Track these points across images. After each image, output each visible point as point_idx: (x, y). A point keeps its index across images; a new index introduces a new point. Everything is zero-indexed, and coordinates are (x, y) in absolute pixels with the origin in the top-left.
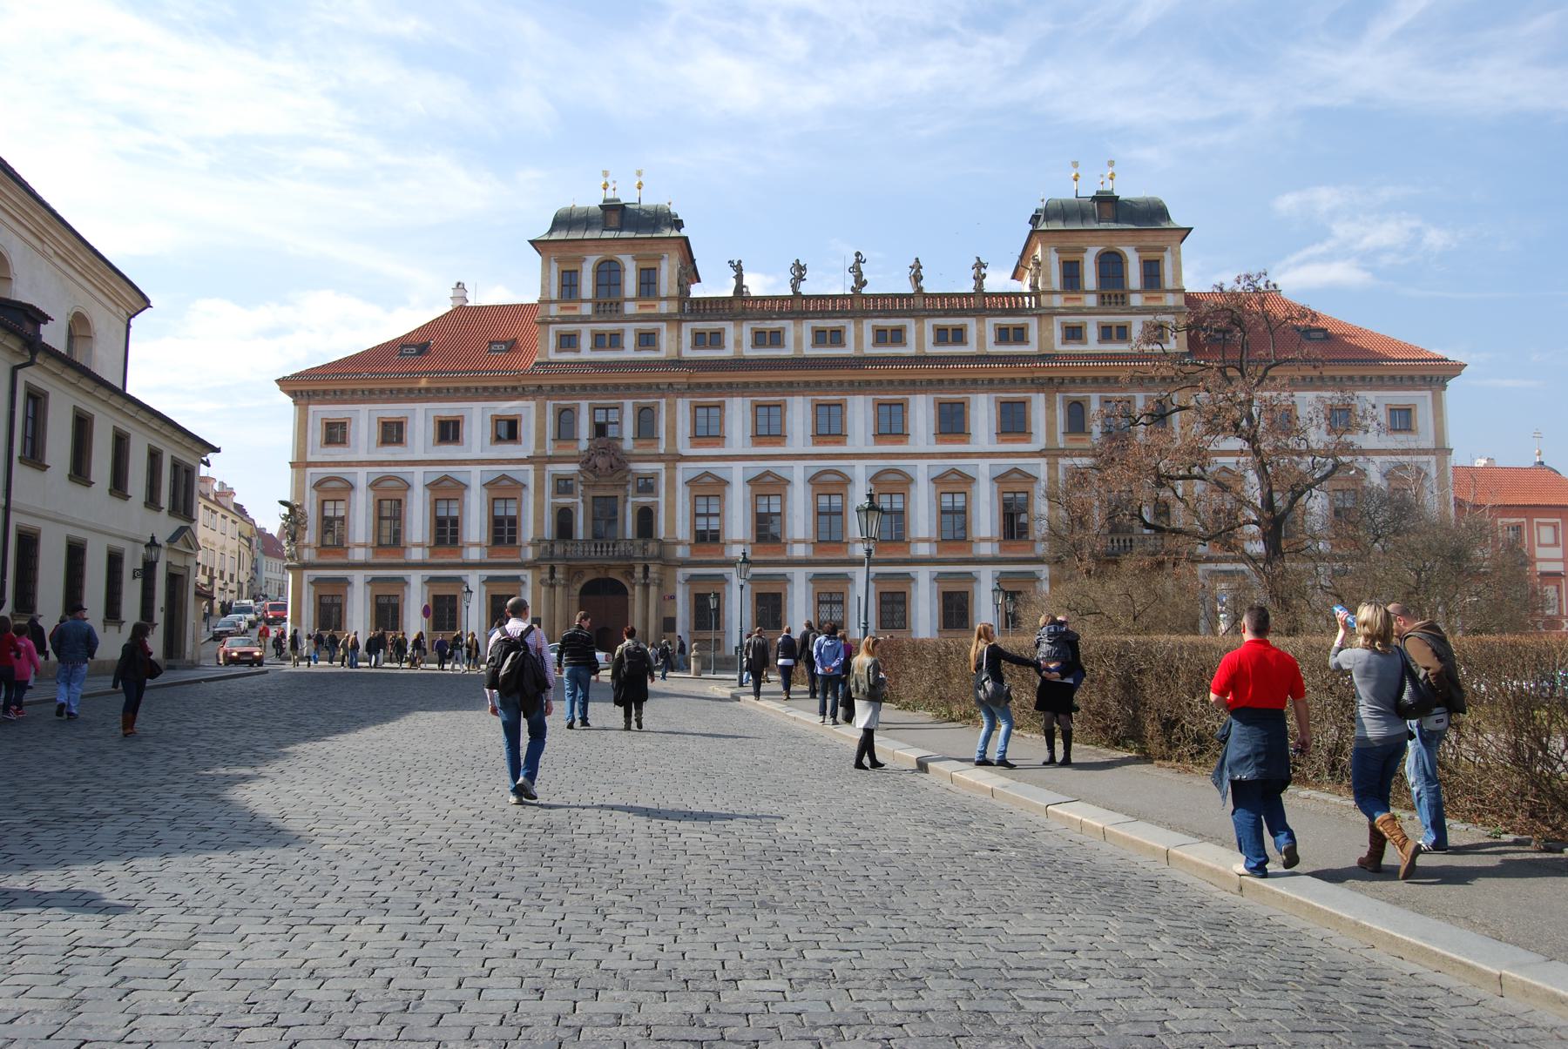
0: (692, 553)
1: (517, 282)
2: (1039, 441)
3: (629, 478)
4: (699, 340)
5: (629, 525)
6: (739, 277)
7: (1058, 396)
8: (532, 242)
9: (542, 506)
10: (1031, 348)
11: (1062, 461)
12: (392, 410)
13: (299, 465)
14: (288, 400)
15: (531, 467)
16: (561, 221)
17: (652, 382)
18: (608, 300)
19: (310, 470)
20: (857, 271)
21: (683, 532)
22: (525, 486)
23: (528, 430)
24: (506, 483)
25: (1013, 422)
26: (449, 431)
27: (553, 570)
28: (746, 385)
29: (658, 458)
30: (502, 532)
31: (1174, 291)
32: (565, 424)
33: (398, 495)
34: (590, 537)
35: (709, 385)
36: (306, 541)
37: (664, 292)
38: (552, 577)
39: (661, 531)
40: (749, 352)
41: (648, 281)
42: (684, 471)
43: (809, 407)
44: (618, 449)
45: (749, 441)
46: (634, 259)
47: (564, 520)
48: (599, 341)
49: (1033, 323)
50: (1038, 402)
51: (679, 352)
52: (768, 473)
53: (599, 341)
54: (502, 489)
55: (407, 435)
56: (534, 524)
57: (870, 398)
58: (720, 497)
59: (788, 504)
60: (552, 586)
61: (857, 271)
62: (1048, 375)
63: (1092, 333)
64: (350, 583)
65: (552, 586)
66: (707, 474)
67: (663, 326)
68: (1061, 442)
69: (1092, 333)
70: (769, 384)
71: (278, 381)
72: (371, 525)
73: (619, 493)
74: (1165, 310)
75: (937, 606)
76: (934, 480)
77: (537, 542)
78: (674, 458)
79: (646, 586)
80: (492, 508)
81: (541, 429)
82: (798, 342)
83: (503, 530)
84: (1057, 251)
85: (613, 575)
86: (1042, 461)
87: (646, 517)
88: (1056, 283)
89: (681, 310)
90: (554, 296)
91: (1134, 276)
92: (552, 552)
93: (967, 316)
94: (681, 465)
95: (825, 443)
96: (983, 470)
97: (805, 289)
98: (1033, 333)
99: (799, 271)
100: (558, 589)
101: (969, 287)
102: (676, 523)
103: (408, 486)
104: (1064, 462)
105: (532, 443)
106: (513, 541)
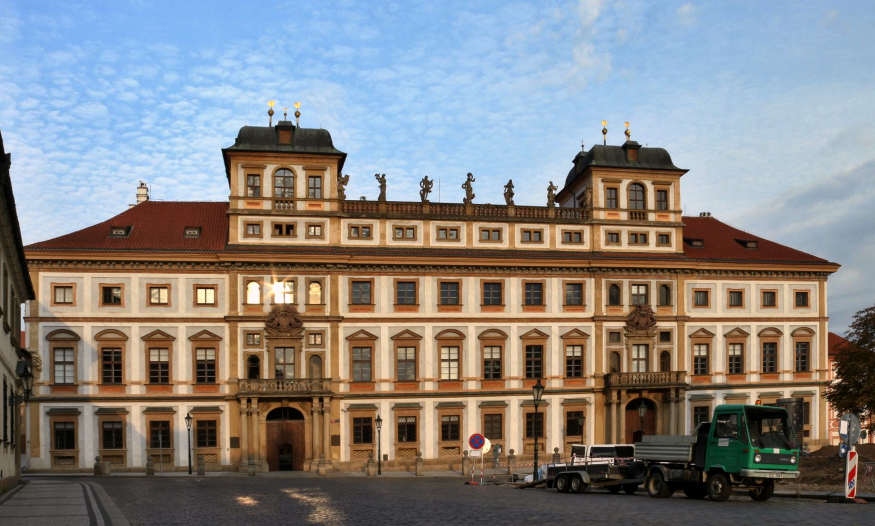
0: (351, 389)
3: (303, 334)
7: (604, 281)
9: (236, 355)
10: (586, 247)
12: (110, 278)
15: (226, 325)
18: (284, 201)
21: (344, 373)
24: (205, 336)
25: (575, 298)
27: (249, 401)
29: (326, 319)
31: (675, 212)
34: (273, 377)
36: (41, 380)
37: (327, 195)
39: (328, 374)
42: (344, 330)
43: (436, 284)
44: (296, 313)
45: (392, 308)
47: (253, 363)
49: (587, 230)
50: (590, 284)
51: (339, 241)
52: (407, 331)
56: (230, 369)
57: (479, 278)
58: (371, 349)
59: (421, 353)
60: (249, 414)
62: (595, 264)
63: (625, 238)
64: (79, 413)
65: (249, 414)
66: (363, 332)
69: (625, 238)
73: (296, 345)
77: (234, 382)
78: (336, 320)
79: (322, 413)
80: (195, 355)
83: (205, 373)
94: (342, 325)
95: (448, 310)
96: (514, 332)
102: (340, 367)
103: (125, 338)
105: (227, 306)
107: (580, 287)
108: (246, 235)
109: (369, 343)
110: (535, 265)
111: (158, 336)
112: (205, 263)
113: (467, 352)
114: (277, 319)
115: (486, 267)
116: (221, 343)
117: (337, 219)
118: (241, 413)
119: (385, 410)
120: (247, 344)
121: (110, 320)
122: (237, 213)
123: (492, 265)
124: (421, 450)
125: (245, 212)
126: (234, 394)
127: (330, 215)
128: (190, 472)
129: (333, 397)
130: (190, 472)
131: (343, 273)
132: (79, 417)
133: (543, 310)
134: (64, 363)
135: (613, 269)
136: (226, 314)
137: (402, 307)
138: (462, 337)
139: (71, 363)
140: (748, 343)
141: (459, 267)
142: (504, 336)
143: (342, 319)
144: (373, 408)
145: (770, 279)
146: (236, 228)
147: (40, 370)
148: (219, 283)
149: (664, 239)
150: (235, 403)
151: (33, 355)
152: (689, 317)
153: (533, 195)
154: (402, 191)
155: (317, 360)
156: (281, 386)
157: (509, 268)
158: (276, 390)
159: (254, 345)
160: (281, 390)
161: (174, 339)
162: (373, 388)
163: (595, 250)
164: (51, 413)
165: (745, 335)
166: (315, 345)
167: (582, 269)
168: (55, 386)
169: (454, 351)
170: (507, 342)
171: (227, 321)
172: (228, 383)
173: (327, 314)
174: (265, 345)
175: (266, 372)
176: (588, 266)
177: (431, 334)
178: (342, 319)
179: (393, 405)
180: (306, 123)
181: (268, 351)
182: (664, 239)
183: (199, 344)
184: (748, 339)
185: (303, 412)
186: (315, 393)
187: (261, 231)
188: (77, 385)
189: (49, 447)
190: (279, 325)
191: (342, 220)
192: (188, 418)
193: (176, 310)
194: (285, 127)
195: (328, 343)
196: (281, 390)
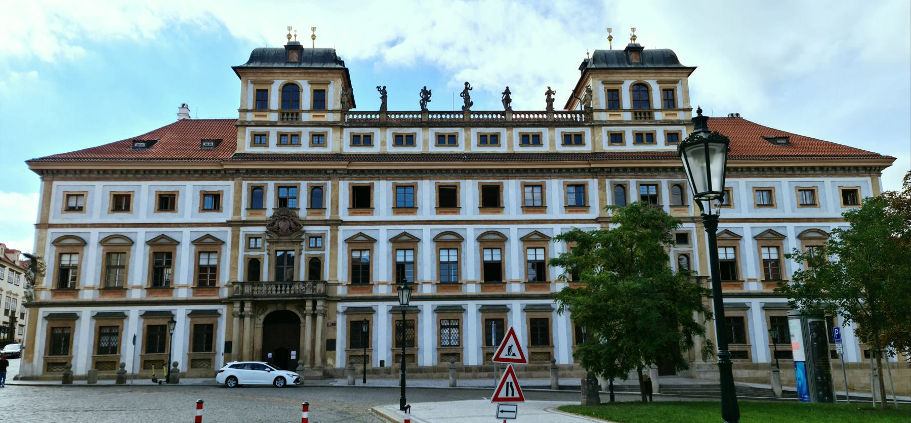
0: (349, 292)
1: (225, 101)
3: (303, 237)
5: (302, 273)
6: (384, 98)
7: (607, 181)
8: (235, 69)
9: (237, 258)
10: (587, 148)
13: (42, 225)
14: (37, 177)
15: (229, 229)
16: (258, 56)
19: (51, 230)
20: (466, 94)
22: (223, 243)
23: (228, 202)
24: (209, 240)
26: (166, 202)
28: (389, 171)
29: (325, 223)
31: (684, 110)
32: (257, 199)
33: (124, 249)
34: (272, 279)
35: (362, 171)
36: (44, 285)
38: (242, 309)
39: (327, 276)
42: (343, 233)
45: (391, 211)
46: (310, 83)
47: (254, 266)
48: (283, 139)
49: (587, 132)
50: (593, 185)
51: (341, 149)
52: (405, 234)
53: (283, 139)
54: (207, 245)
55: (133, 205)
56: (230, 270)
60: (242, 317)
61: (466, 94)
62: (599, 166)
63: (629, 138)
65: (242, 317)
66: (361, 234)
67: (330, 130)
69: (629, 138)
70: (405, 171)
73: (297, 248)
74: (679, 123)
78: (336, 223)
79: (314, 316)
81: (238, 202)
82: (426, 143)
83: (206, 277)
84: (604, 83)
85: (291, 308)
87: (315, 266)
88: (603, 106)
89: (343, 119)
90: (250, 107)
92: (243, 291)
93: (543, 126)
94: (341, 228)
95: (445, 213)
97: (430, 107)
99: (426, 95)
100: (247, 320)
101: (543, 107)
102: (338, 271)
105: (231, 211)
106: (213, 283)
107: (581, 189)
108: (254, 144)
109: (368, 246)
111: (163, 241)
112: (212, 171)
116: (223, 247)
120: (248, 247)
122: (244, 125)
129: (331, 300)
131: (344, 178)
132: (77, 322)
135: (617, 169)
136: (229, 219)
137: (400, 210)
141: (455, 171)
143: (342, 223)
146: (244, 138)
147: (44, 275)
148: (225, 189)
151: (38, 261)
154: (404, 101)
157: (506, 170)
159: (256, 248)
160: (279, 293)
161: (178, 243)
162: (371, 292)
163: (597, 151)
164: (50, 317)
166: (316, 248)
167: (583, 170)
169: (453, 252)
170: (507, 244)
171: (230, 226)
173: (328, 218)
176: (588, 166)
178: (342, 223)
179: (390, 308)
181: (269, 254)
183: (201, 248)
185: (300, 315)
186: (308, 296)
187: (267, 140)
189: (43, 353)
193: (182, 216)
196: (279, 293)
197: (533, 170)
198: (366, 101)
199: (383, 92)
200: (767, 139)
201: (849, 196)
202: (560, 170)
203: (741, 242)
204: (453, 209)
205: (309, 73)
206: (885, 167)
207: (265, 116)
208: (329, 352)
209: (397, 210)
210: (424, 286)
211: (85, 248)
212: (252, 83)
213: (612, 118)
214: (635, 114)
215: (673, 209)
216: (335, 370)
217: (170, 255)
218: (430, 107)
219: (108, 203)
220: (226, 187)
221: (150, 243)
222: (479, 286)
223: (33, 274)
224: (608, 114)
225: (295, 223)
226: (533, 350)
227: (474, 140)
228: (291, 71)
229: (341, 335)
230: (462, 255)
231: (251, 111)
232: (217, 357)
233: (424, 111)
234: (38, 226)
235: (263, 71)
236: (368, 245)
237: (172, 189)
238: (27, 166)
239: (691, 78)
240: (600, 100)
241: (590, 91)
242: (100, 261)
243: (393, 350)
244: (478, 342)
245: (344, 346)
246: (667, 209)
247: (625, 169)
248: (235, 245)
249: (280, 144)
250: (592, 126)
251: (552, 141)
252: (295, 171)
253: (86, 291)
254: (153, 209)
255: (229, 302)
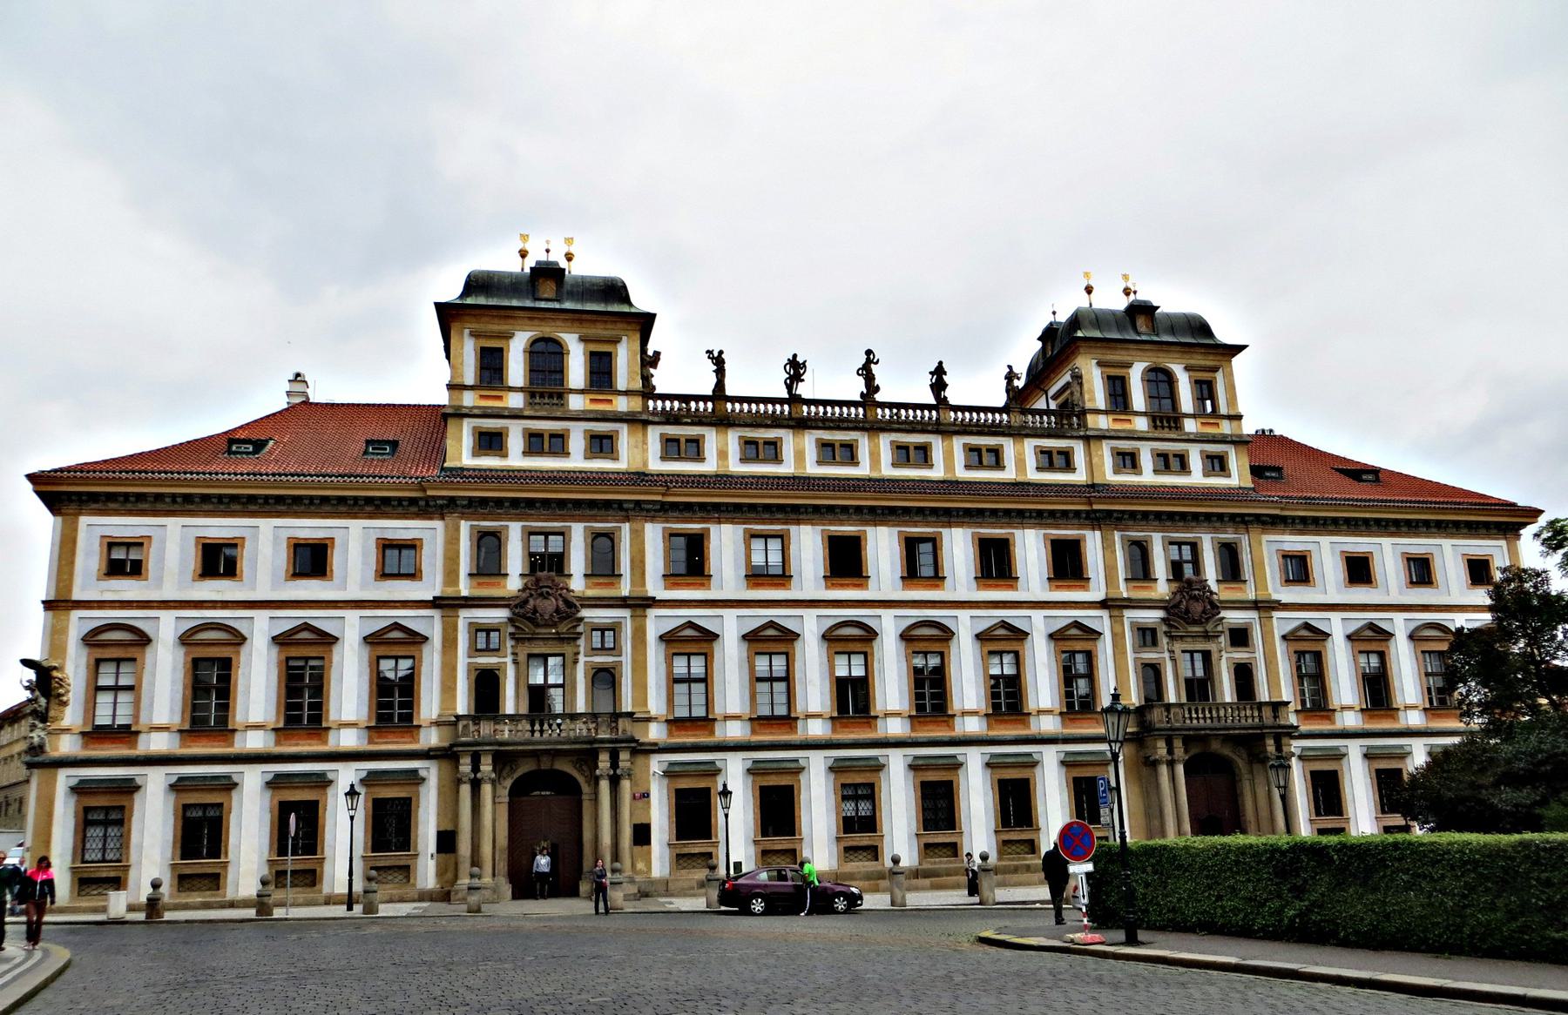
2: (1096, 593)
3: (580, 629)
4: (671, 448)
6: (720, 372)
7: (1117, 535)
9: (454, 669)
10: (1079, 476)
11: (1128, 614)
15: (436, 614)
17: (613, 503)
19: (76, 614)
20: (866, 372)
21: (656, 704)
24: (396, 634)
29: (622, 603)
30: (299, 707)
31: (1230, 418)
34: (524, 710)
35: (688, 507)
37: (621, 383)
38: (476, 768)
40: (736, 467)
41: (601, 373)
42: (657, 623)
43: (819, 539)
46: (584, 339)
47: (486, 686)
48: (535, 445)
49: (1079, 449)
50: (1092, 542)
51: (645, 463)
52: (771, 624)
53: (535, 445)
55: (244, 565)
56: (441, 696)
57: (896, 530)
58: (708, 657)
59: (798, 665)
60: (476, 785)
61: (866, 372)
63: (1146, 461)
65: (476, 785)
66: (691, 625)
67: (624, 429)
68: (1124, 591)
71: (32, 478)
72: (179, 696)
73: (568, 650)
74: (1223, 440)
75: (962, 805)
76: (978, 637)
77: (450, 723)
78: (640, 604)
79: (615, 781)
82: (800, 456)
83: (393, 702)
86: (1105, 614)
90: (469, 378)
91: (1186, 402)
94: (652, 613)
95: (842, 586)
97: (804, 390)
98: (1079, 458)
99: (796, 370)
100: (487, 789)
102: (650, 691)
104: (1130, 615)
105: (439, 578)
109: (703, 647)
110: (995, 512)
112: (400, 500)
113: (882, 661)
114: (532, 602)
115: (907, 510)
116: (426, 649)
117: (640, 426)
118: (459, 782)
119: (735, 772)
120: (474, 650)
121: (213, 605)
122: (460, 414)
123: (921, 511)
124: (806, 854)
125: (476, 411)
126: (446, 744)
127: (630, 419)
128: (350, 908)
130: (350, 908)
131: (653, 519)
132: (137, 797)
133: (1013, 587)
134: (116, 689)
135: (1133, 515)
136: (438, 594)
138: (870, 635)
139: (130, 688)
140: (1392, 650)
141: (859, 509)
142: (946, 634)
144: (713, 771)
145: (1417, 535)
146: (460, 440)
147: (65, 704)
149: (1217, 464)
150: (446, 765)
152: (1278, 602)
153: (976, 387)
154: (759, 378)
155: (605, 678)
156: (537, 727)
158: (528, 735)
159: (488, 650)
160: (537, 735)
162: (712, 733)
164: (80, 789)
165: (1387, 636)
166: (603, 649)
167: (1077, 513)
168: (97, 734)
170: (953, 644)
172: (437, 724)
174: (509, 651)
175: (510, 703)
177: (815, 629)
178: (653, 602)
179: (749, 764)
180: (587, 266)
181: (515, 662)
182: (1217, 464)
184: (1392, 643)
185: (581, 779)
186: (602, 741)
188: (137, 733)
190: (535, 611)
191: (650, 428)
192: (352, 793)
194: (548, 273)
195: (627, 647)
196: (537, 735)
197: (994, 512)
198: (680, 374)
199: (719, 362)
200: (1341, 471)
201: (1478, 571)
202: (1040, 513)
203: (1329, 644)
204: (856, 581)
205: (581, 321)
206: (1524, 525)
207: (500, 398)
208: (638, 849)
209: (754, 580)
210: (967, 719)
211: (149, 650)
212: (473, 334)
213: (1118, 426)
214: (1154, 421)
215: (1222, 586)
216: (652, 882)
217: (226, 665)
218: (804, 390)
219: (193, 560)
220: (429, 532)
221: (280, 641)
222: (907, 722)
223: (43, 701)
224: (1111, 418)
225: (566, 602)
226: (1006, 837)
227: (886, 455)
228: (548, 315)
229: (660, 816)
230: (876, 665)
231: (471, 388)
232: (420, 861)
233: (794, 400)
234: (48, 605)
235: (495, 313)
236: (705, 645)
237: (321, 534)
238: (29, 486)
239: (1238, 361)
240: (1096, 393)
241: (1077, 377)
242: (180, 675)
243: (756, 842)
244: (909, 825)
245: (666, 837)
246: (1214, 587)
247: (1146, 515)
248: (449, 643)
249: (529, 451)
250: (1087, 439)
251: (1021, 461)
252: (562, 503)
253: (154, 735)
254: (283, 574)
255: (446, 755)
